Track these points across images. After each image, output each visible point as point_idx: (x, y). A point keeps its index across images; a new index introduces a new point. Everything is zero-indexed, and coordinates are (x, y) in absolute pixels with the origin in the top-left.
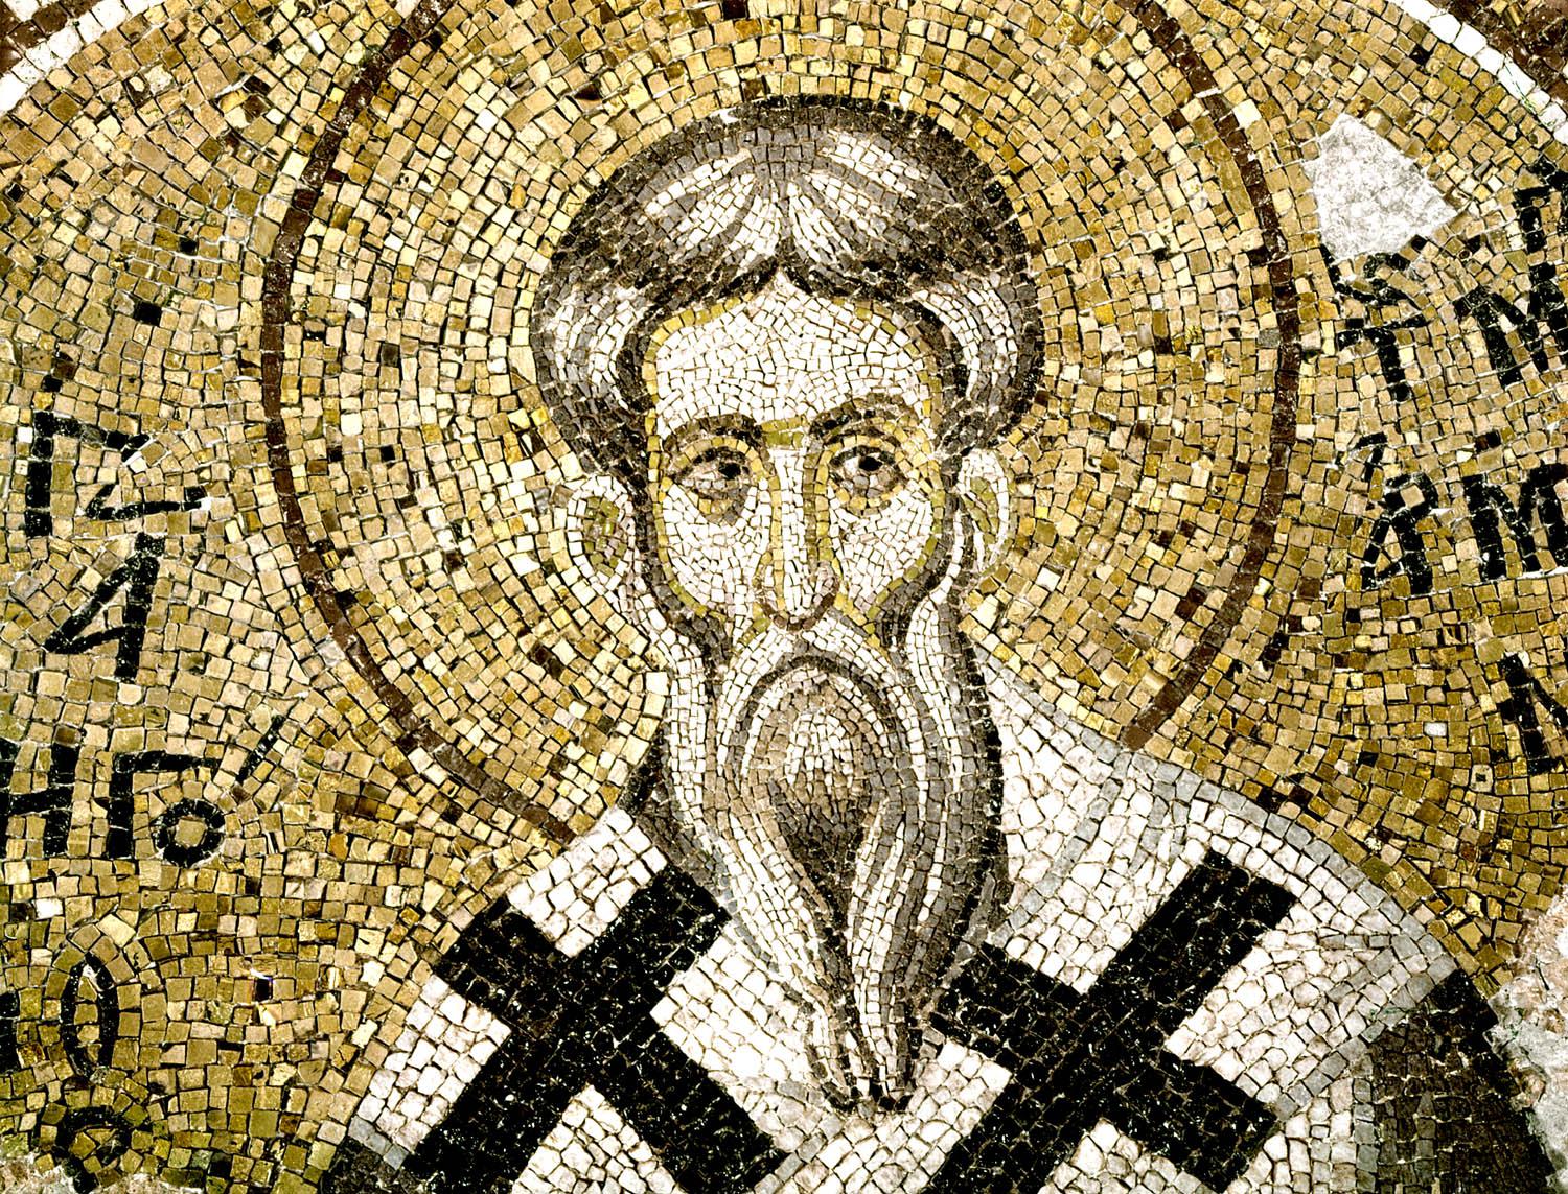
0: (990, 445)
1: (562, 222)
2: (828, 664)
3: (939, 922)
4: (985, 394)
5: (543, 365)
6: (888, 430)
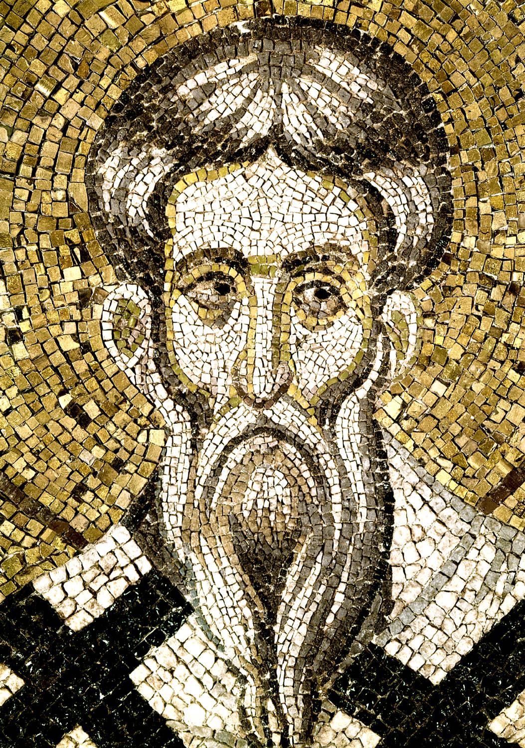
0: (408, 289)
1: (115, 94)
2: (280, 434)
3: (341, 626)
4: (407, 252)
5: (94, 198)
6: (337, 270)
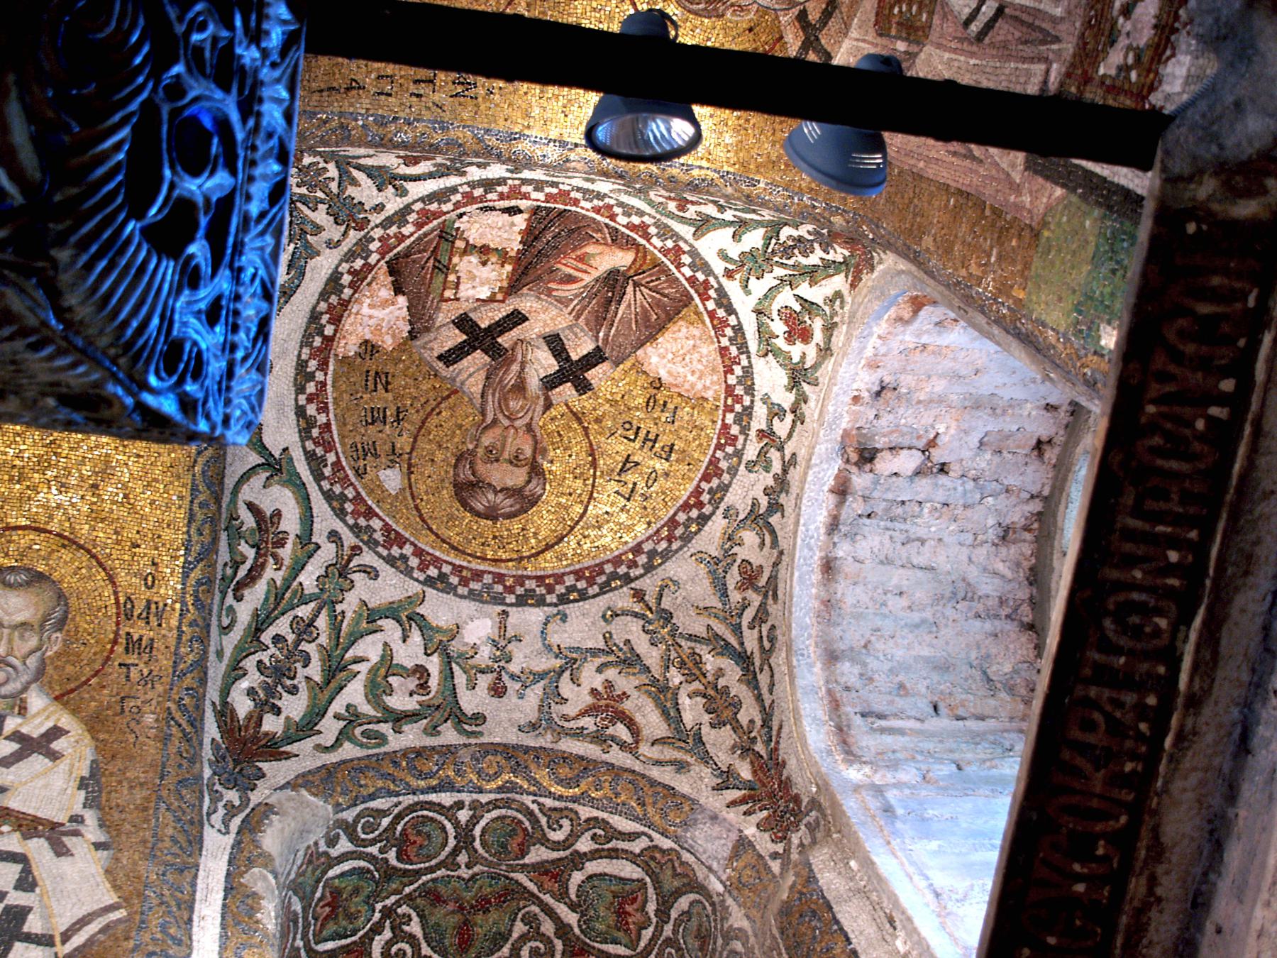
2: (508, 418)
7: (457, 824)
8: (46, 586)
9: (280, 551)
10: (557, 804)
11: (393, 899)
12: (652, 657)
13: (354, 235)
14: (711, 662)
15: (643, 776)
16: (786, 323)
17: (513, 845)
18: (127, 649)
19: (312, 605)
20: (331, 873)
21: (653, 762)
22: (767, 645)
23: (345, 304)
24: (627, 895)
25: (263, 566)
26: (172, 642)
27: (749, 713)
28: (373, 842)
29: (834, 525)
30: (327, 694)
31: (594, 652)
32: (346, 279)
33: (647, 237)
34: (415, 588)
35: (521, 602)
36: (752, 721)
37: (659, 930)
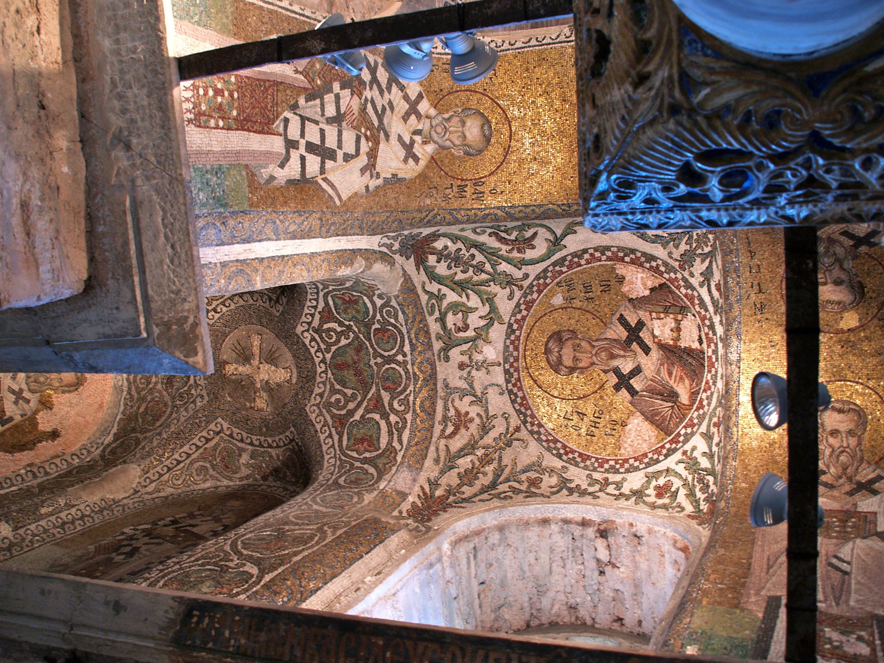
7: (395, 355)
8: (485, 144)
9: (515, 251)
10: (411, 402)
11: (356, 329)
12: (488, 440)
13: (676, 265)
14: (489, 469)
15: (430, 443)
16: (665, 485)
17: (388, 384)
18: (459, 186)
19: (492, 271)
20: (365, 298)
21: (438, 446)
22: (502, 496)
23: (641, 265)
24: (371, 442)
25: (507, 244)
26: (465, 207)
27: (468, 491)
28: (382, 316)
29: (566, 521)
30: (450, 284)
31: (486, 411)
32: (654, 264)
33: (697, 409)
34: (506, 319)
35: (506, 372)
36: (464, 493)
37: (357, 460)
